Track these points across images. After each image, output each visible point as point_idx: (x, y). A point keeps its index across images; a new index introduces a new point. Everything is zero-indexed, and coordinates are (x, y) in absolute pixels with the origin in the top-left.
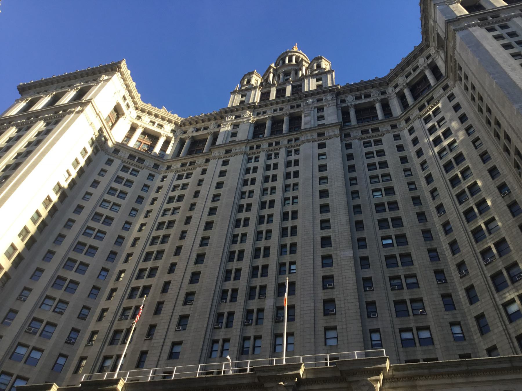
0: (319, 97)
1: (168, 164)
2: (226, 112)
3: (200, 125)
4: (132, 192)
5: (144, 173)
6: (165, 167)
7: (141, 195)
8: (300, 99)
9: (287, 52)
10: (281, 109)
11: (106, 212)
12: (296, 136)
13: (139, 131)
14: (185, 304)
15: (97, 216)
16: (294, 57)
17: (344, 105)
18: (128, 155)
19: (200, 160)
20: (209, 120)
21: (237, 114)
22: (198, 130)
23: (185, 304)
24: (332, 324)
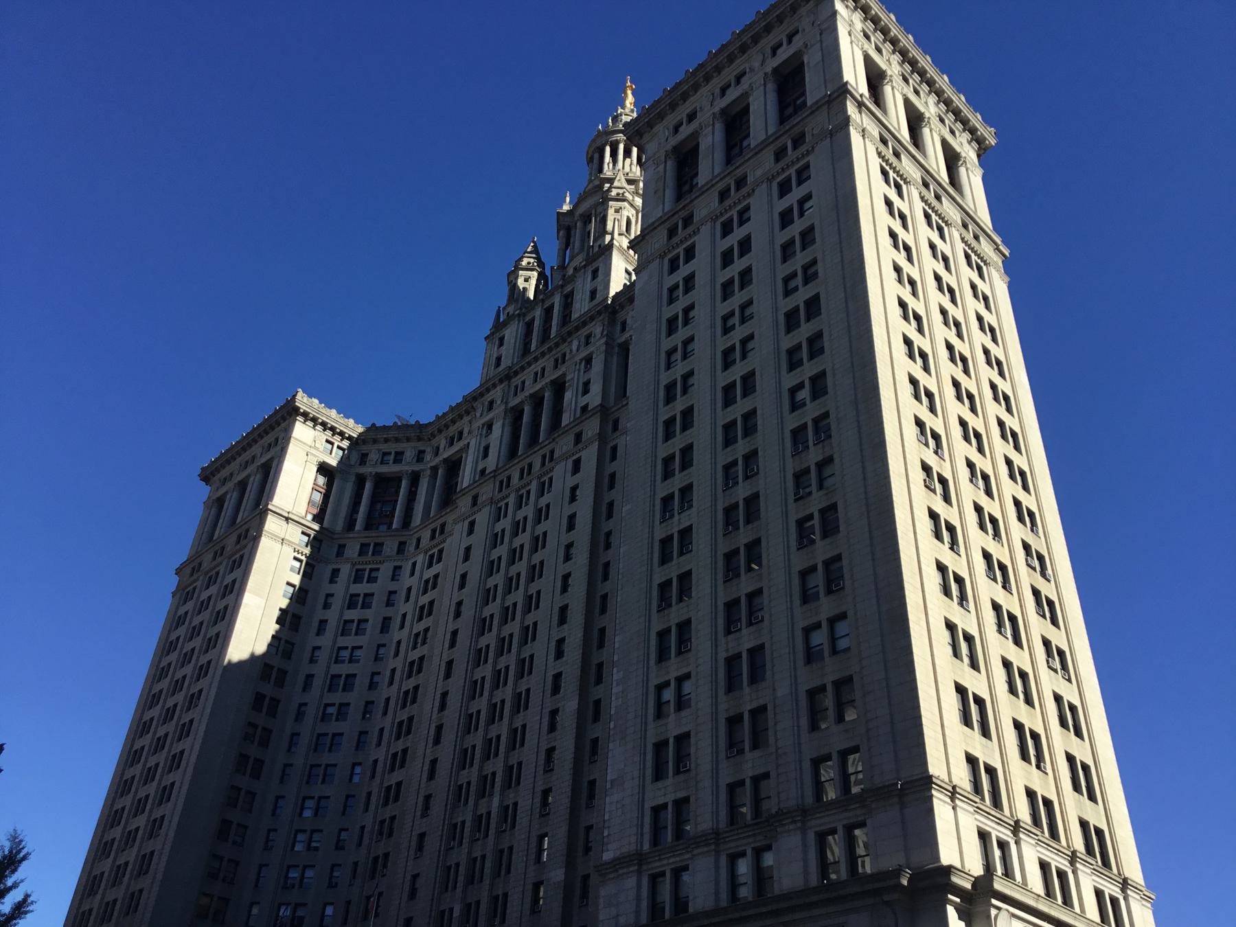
0: (584, 332)
1: (417, 535)
2: (475, 399)
3: (453, 430)
4: (373, 615)
5: (385, 570)
6: (414, 542)
7: (388, 615)
8: (564, 341)
9: (600, 134)
10: (543, 369)
11: (344, 669)
12: (550, 447)
13: (368, 486)
14: (423, 816)
15: (333, 683)
16: (608, 149)
17: (623, 339)
18: (358, 547)
19: (450, 519)
20: (461, 417)
21: (488, 397)
22: (452, 444)
23: (423, 816)
24: (545, 830)
